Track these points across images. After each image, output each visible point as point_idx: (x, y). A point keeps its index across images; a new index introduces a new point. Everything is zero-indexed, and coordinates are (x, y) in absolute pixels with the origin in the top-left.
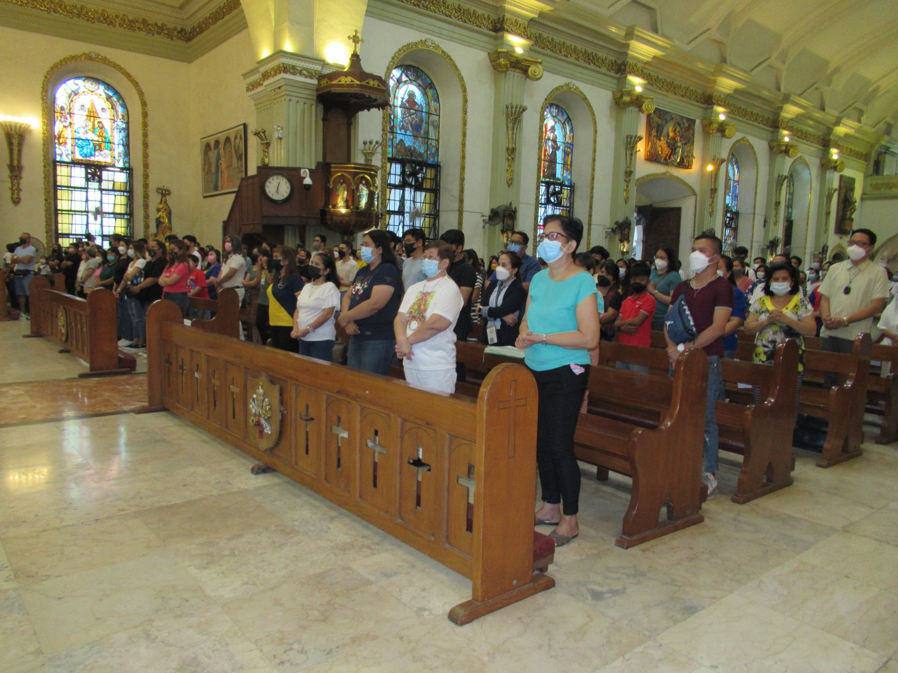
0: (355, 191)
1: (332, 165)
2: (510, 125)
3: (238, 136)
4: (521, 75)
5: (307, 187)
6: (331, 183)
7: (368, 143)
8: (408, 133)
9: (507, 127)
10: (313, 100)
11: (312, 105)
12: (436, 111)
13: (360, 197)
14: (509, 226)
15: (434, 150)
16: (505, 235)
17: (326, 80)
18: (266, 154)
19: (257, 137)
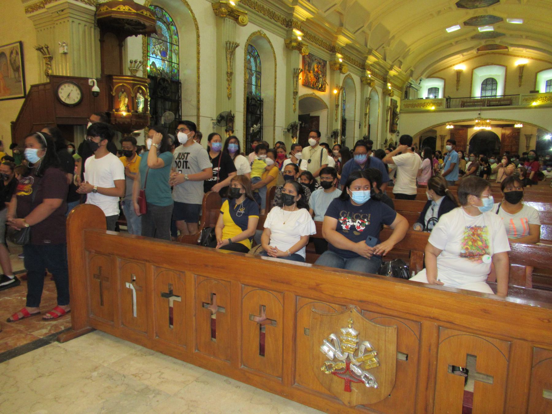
0: (134, 99)
1: (114, 77)
2: (229, 56)
3: (14, 52)
4: (233, 21)
5: (96, 94)
6: (114, 91)
7: (134, 62)
8: (158, 57)
9: (227, 58)
10: (92, 23)
11: (91, 27)
12: (176, 42)
13: (138, 103)
14: (230, 127)
15: (176, 71)
16: (228, 133)
17: (106, 7)
18: (50, 66)
19: (39, 52)
